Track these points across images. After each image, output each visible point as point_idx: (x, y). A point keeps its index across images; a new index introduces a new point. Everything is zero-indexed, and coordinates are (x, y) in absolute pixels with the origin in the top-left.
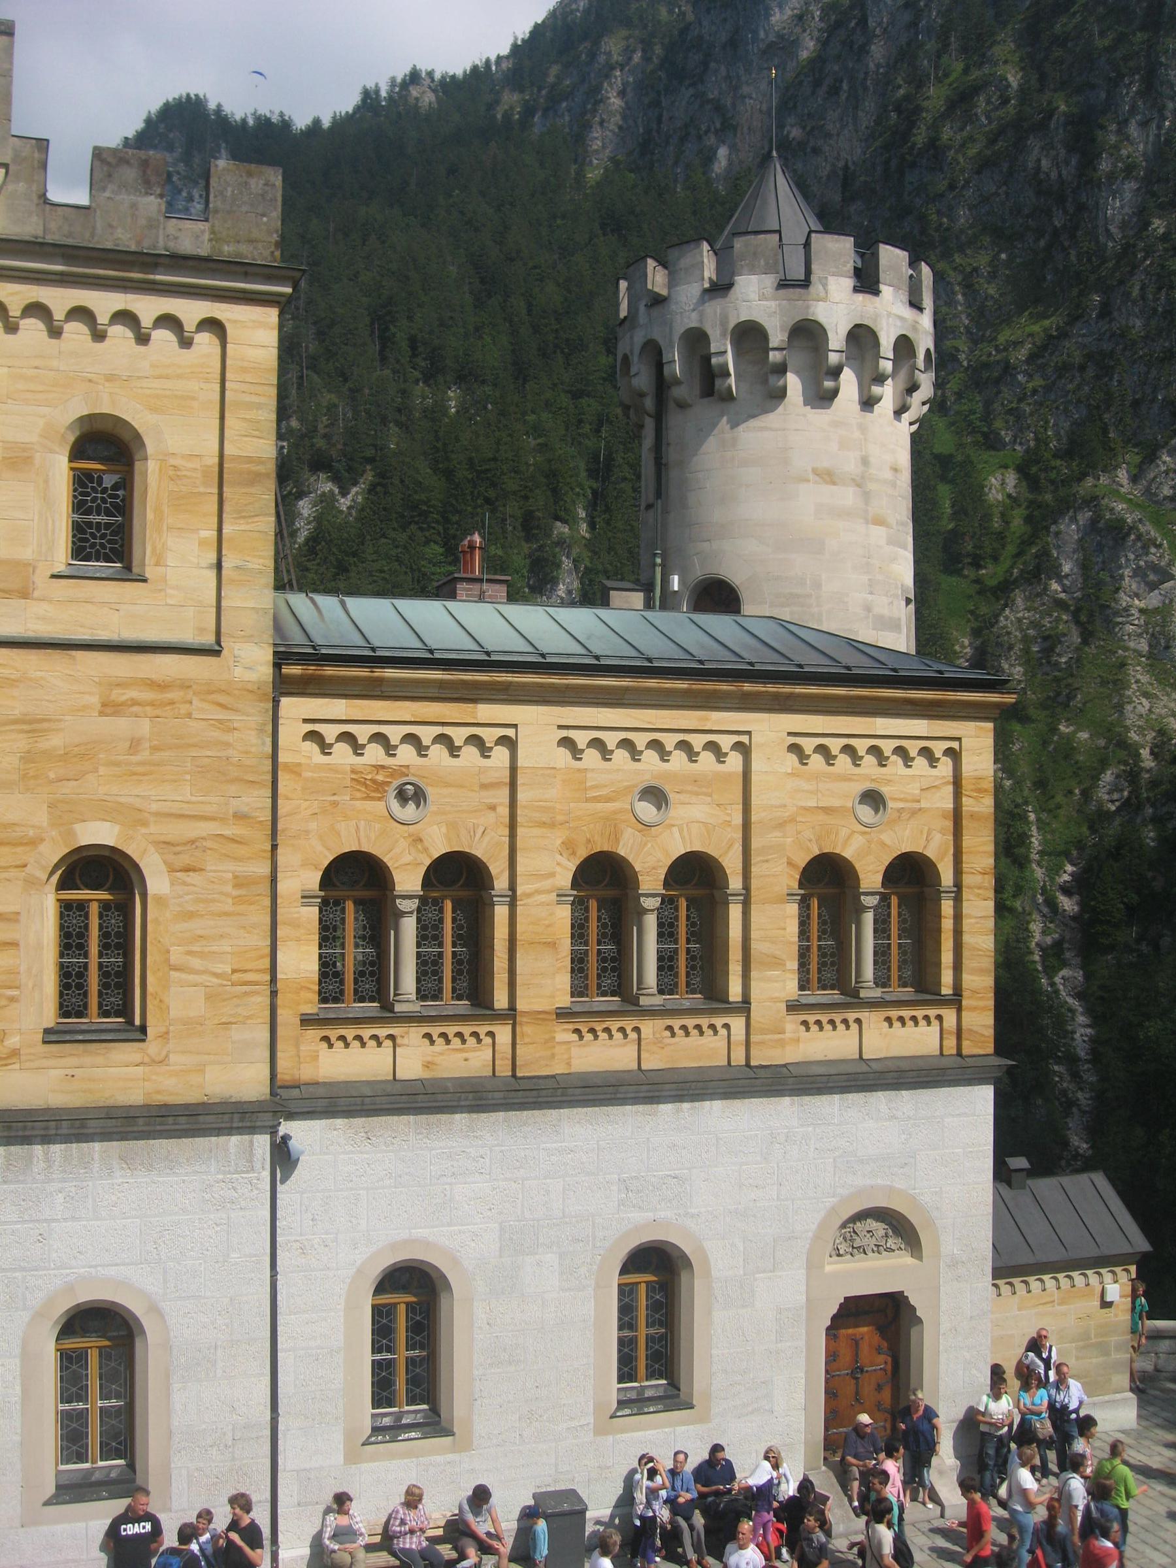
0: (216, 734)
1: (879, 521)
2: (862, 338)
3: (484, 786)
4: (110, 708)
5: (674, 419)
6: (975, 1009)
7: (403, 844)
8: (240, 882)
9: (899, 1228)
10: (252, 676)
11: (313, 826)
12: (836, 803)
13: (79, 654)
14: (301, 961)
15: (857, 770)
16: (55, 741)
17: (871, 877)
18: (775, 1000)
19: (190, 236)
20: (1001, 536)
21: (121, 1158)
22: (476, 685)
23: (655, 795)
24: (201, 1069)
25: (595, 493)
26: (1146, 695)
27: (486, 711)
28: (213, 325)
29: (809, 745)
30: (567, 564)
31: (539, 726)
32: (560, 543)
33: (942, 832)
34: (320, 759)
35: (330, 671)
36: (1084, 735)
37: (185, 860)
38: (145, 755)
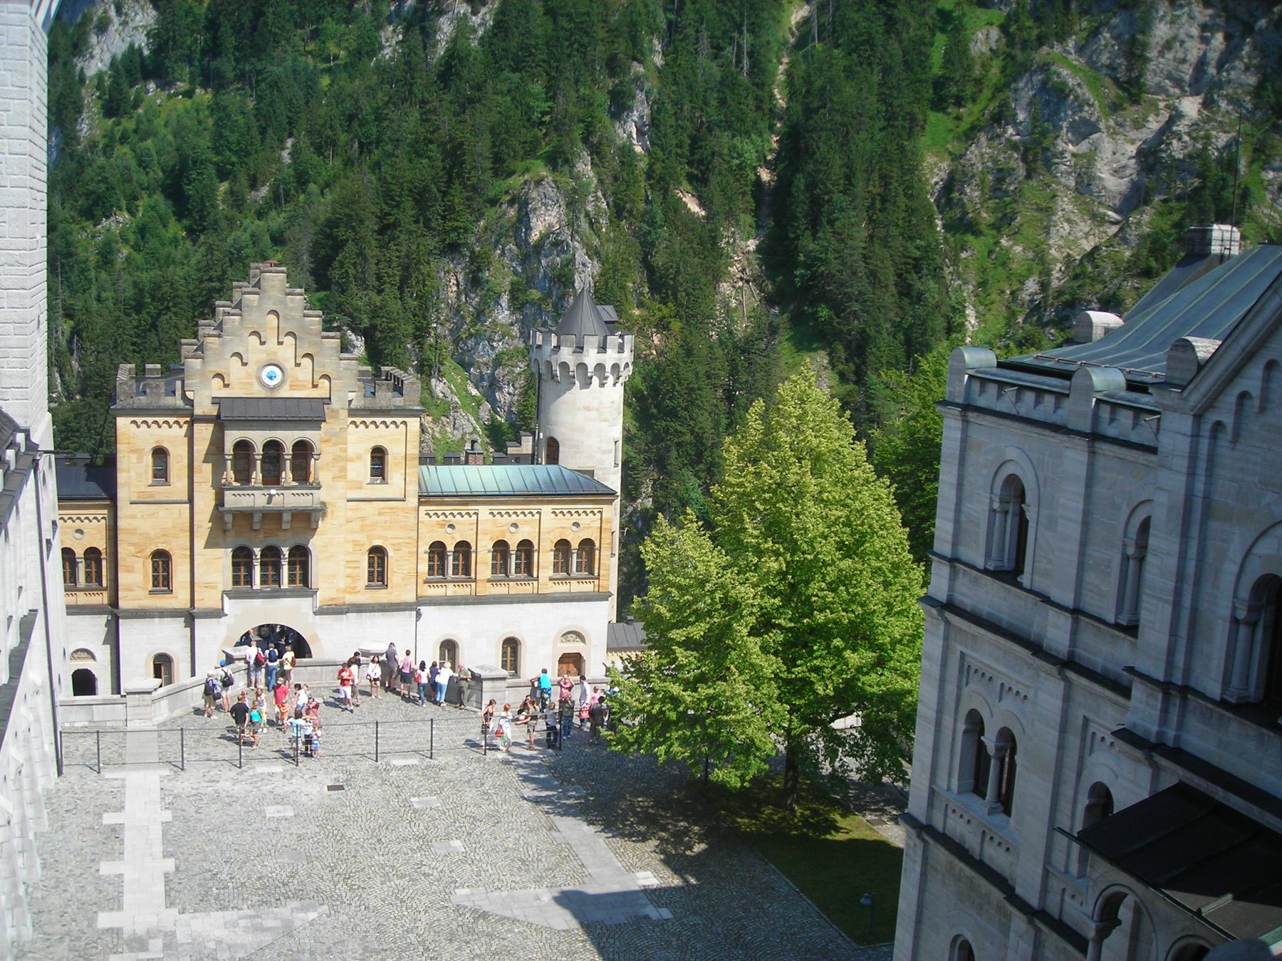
1: (605, 421)
2: (600, 367)
4: (380, 514)
5: (543, 383)
9: (580, 636)
14: (424, 567)
17: (575, 545)
19: (399, 401)
20: (979, 82)
23: (515, 525)
25: (670, 24)
26: (1069, 221)
28: (405, 423)
30: (640, 96)
31: (484, 510)
32: (637, 78)
36: (1018, 249)
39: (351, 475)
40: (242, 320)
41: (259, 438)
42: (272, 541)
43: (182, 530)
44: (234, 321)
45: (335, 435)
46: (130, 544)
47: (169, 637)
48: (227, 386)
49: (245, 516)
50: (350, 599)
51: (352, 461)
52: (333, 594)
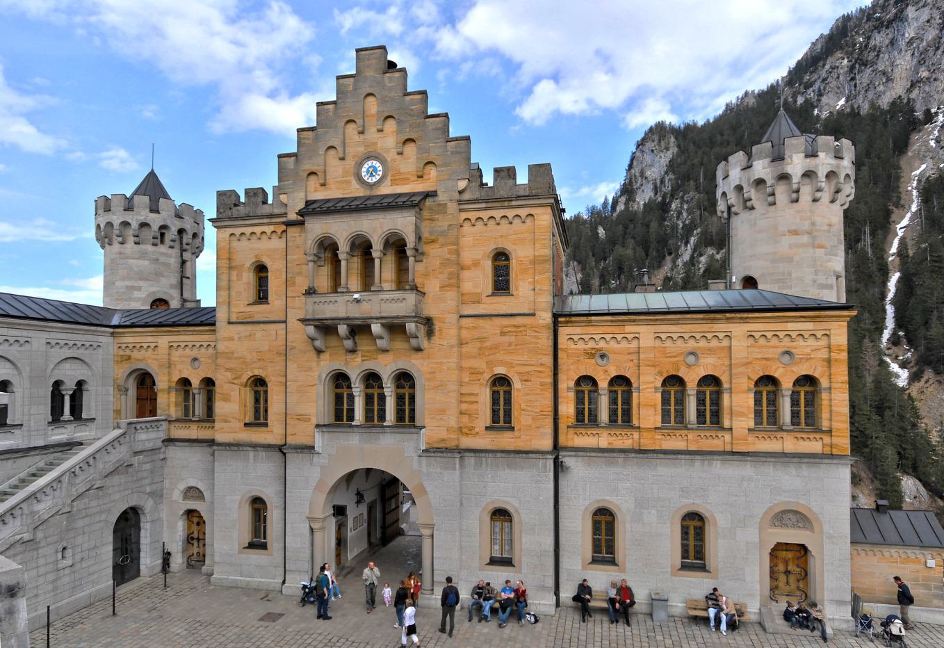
0: (533, 340)
3: (629, 354)
4: (503, 334)
6: (839, 436)
7: (601, 373)
8: (542, 384)
10: (544, 322)
11: (572, 367)
12: (771, 356)
13: (493, 318)
14: (568, 409)
15: (781, 344)
16: (487, 344)
18: (745, 428)
21: (508, 466)
22: (623, 321)
24: (531, 440)
27: (628, 328)
29: (757, 335)
33: (822, 366)
34: (573, 346)
35: (574, 319)
37: (525, 378)
38: (513, 347)
39: (467, 286)
40: (336, 109)
41: (341, 229)
42: (371, 365)
43: (279, 354)
44: (328, 111)
45: (443, 233)
46: (227, 370)
47: (256, 476)
48: (323, 185)
49: (327, 328)
50: (467, 442)
51: (468, 268)
52: (443, 434)
